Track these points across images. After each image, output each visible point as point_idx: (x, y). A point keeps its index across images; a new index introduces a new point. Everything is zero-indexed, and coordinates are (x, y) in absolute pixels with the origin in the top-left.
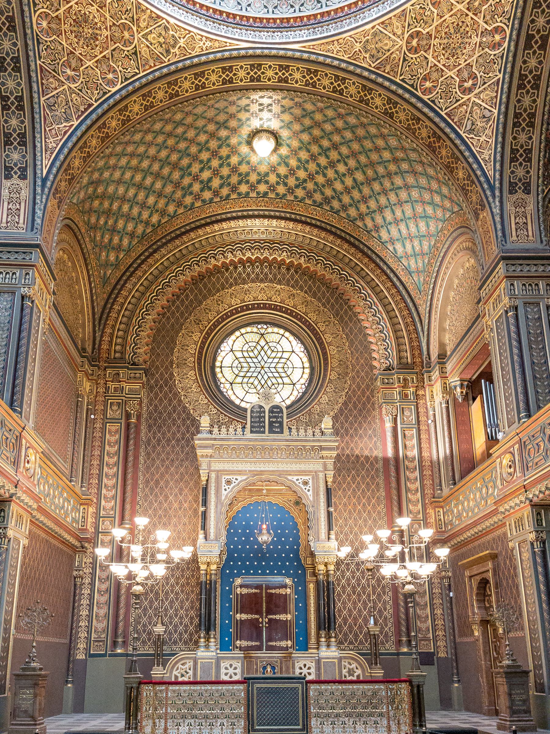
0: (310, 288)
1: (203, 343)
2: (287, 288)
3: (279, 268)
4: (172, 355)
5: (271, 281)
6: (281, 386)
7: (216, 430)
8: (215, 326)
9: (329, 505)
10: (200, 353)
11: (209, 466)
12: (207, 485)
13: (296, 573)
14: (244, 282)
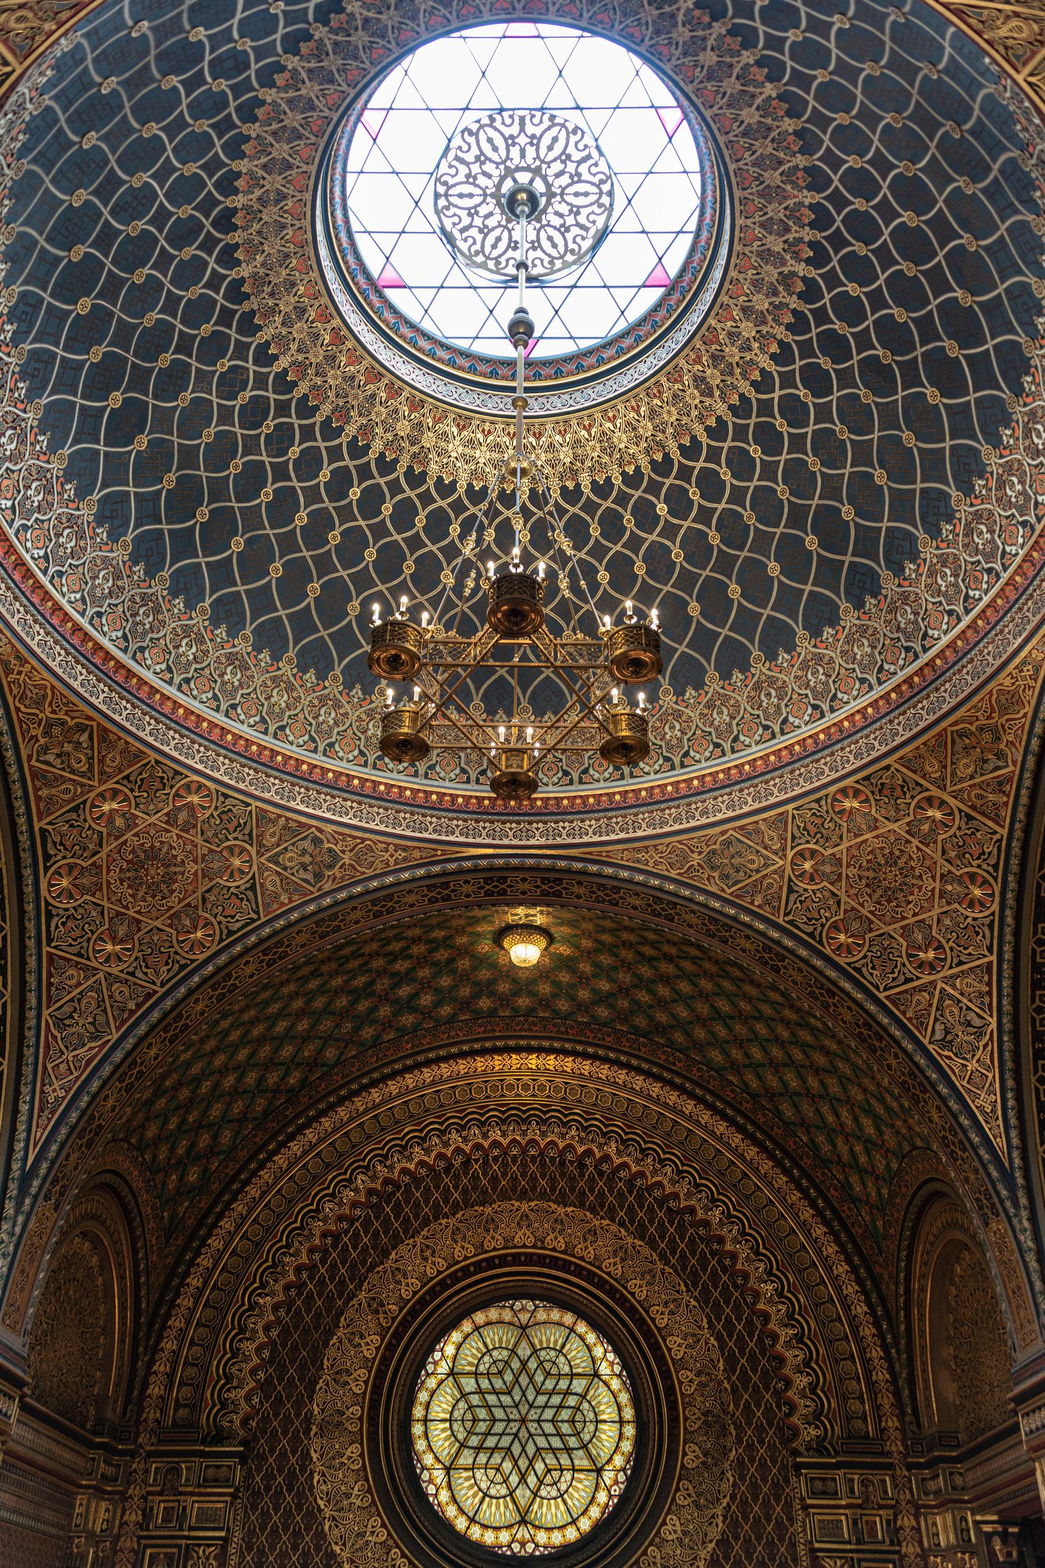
0: (631, 1212)
1: (385, 1361)
2: (579, 1213)
4: (311, 1398)
5: (543, 1196)
6: (568, 1475)
8: (414, 1312)
10: (377, 1389)
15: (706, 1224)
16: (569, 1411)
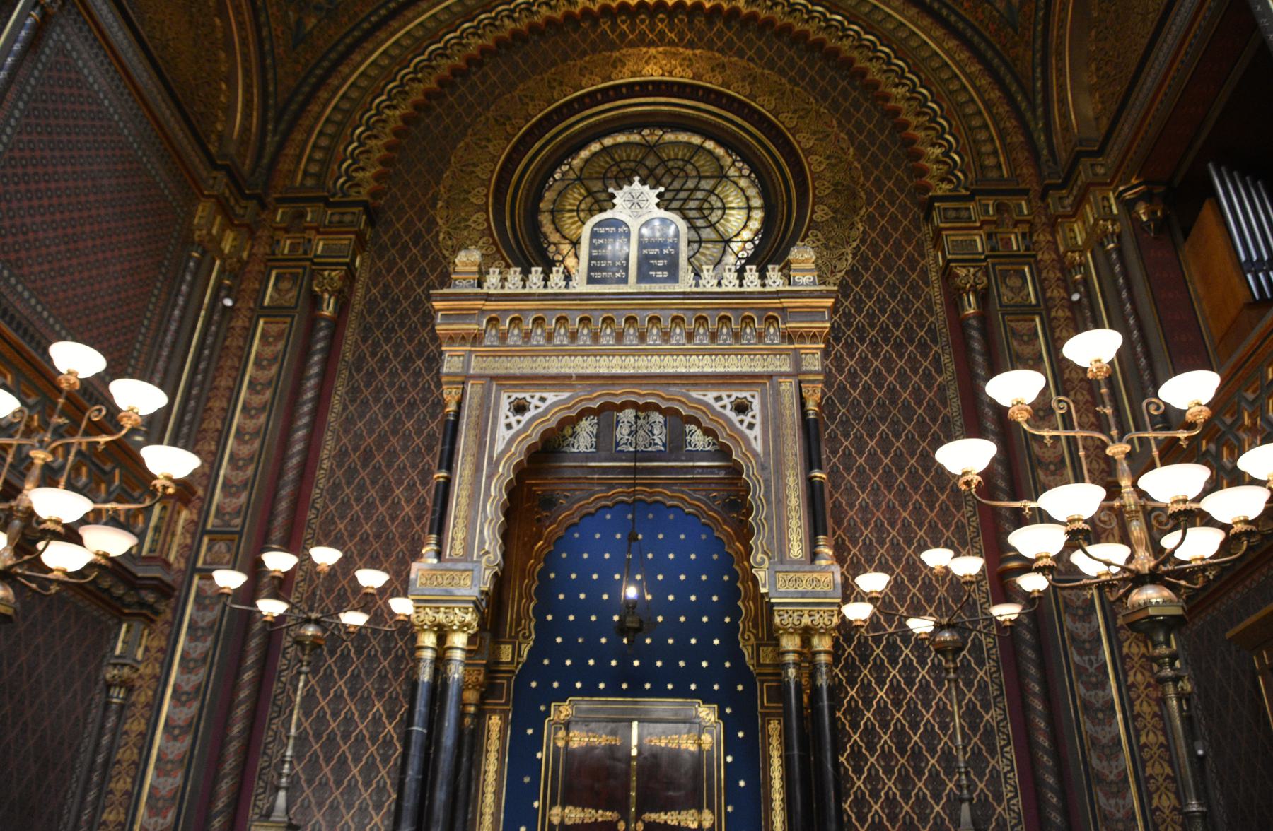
2: (707, 53)
3: (691, 22)
5: (671, 43)
7: (493, 279)
9: (812, 460)
11: (467, 364)
12: (458, 414)
13: (728, 688)
14: (612, 46)
15: (835, 52)
16: (697, 203)
